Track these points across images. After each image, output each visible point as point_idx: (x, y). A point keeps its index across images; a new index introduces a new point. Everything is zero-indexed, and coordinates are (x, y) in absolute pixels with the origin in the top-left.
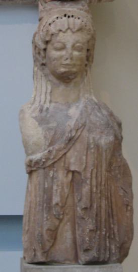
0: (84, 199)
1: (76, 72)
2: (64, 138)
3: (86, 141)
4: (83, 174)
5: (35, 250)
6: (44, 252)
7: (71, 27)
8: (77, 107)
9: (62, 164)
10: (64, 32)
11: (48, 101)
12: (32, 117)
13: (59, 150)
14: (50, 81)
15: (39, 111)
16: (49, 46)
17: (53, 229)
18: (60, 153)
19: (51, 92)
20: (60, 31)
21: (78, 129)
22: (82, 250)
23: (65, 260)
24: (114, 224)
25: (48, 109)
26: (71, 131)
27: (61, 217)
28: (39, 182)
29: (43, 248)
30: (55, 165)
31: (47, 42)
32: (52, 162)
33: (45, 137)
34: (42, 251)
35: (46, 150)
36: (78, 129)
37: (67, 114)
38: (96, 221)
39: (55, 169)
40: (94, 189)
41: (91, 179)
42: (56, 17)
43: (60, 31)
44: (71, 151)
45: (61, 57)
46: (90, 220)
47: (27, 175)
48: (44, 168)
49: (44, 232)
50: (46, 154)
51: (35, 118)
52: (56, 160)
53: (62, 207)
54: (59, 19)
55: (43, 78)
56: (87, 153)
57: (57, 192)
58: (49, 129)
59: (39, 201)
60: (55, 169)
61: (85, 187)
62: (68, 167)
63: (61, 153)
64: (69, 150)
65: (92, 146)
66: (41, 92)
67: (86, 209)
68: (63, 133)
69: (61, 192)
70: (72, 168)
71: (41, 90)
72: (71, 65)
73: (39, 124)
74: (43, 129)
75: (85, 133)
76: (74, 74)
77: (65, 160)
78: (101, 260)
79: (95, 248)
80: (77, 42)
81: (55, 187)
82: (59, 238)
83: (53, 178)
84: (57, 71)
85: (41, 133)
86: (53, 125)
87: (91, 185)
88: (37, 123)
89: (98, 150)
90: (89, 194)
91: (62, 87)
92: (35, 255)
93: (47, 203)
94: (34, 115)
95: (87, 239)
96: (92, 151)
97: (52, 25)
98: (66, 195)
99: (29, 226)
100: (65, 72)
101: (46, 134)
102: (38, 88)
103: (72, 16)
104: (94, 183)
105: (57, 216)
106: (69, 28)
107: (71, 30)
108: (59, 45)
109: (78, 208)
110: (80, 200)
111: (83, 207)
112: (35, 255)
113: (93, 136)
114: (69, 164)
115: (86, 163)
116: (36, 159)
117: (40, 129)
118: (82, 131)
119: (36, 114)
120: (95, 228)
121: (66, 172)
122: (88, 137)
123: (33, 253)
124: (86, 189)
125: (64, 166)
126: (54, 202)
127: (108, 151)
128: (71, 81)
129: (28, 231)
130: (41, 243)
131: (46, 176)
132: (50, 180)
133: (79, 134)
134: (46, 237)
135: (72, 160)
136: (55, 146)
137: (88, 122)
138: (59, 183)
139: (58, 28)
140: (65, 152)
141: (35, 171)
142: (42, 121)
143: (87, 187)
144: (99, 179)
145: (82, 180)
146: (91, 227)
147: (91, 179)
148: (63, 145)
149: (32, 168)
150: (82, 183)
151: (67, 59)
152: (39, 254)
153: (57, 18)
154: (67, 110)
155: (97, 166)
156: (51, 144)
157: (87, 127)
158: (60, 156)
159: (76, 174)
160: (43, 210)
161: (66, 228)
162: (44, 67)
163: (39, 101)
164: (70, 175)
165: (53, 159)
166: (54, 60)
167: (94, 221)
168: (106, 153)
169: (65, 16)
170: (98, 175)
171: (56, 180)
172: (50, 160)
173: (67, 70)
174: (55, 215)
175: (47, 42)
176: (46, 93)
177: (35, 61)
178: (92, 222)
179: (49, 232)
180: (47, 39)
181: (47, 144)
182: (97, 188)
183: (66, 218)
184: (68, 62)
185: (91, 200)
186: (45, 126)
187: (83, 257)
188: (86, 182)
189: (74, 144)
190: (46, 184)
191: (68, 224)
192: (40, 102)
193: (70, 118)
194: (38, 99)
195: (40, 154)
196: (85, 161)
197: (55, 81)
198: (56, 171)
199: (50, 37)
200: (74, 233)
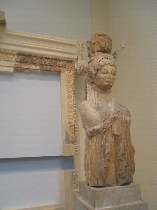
0: (121, 150)
2: (111, 117)
5: (97, 180)
6: (103, 181)
7: (110, 63)
8: (111, 103)
9: (110, 131)
10: (107, 65)
12: (92, 107)
13: (109, 124)
14: (96, 90)
16: (99, 72)
19: (97, 96)
20: (105, 64)
26: (113, 114)
28: (98, 141)
30: (107, 132)
31: (98, 70)
32: (106, 130)
33: (101, 117)
37: (108, 106)
42: (102, 58)
43: (105, 64)
44: (114, 124)
45: (106, 77)
46: (125, 161)
48: (101, 134)
49: (103, 169)
52: (107, 129)
54: (103, 59)
55: (92, 89)
58: (103, 113)
60: (107, 134)
61: (121, 143)
62: (114, 133)
63: (109, 125)
64: (113, 123)
67: (122, 155)
68: (109, 115)
70: (115, 133)
72: (110, 82)
73: (97, 111)
74: (99, 113)
75: (120, 115)
77: (111, 130)
79: (127, 176)
80: (113, 71)
81: (107, 144)
82: (109, 172)
83: (106, 139)
85: (98, 115)
87: (124, 142)
88: (95, 110)
89: (126, 124)
91: (103, 94)
92: (98, 182)
95: (124, 171)
96: (124, 124)
97: (101, 62)
99: (91, 166)
100: (107, 85)
103: (109, 59)
104: (125, 142)
106: (109, 63)
107: (110, 64)
108: (105, 71)
109: (119, 155)
110: (119, 151)
112: (98, 182)
114: (114, 131)
116: (97, 129)
117: (98, 113)
121: (112, 135)
124: (122, 145)
129: (90, 168)
131: (102, 138)
132: (104, 140)
135: (115, 129)
138: (109, 141)
139: (104, 63)
141: (96, 135)
142: (98, 109)
143: (122, 144)
146: (125, 164)
147: (124, 139)
151: (109, 78)
153: (102, 59)
154: (107, 104)
156: (104, 121)
159: (117, 137)
162: (93, 84)
165: (106, 128)
166: (102, 79)
169: (106, 58)
171: (107, 140)
173: (108, 84)
174: (107, 159)
175: (98, 70)
176: (95, 96)
179: (105, 168)
180: (99, 68)
181: (103, 121)
184: (109, 80)
185: (125, 151)
187: (122, 181)
189: (115, 121)
193: (110, 108)
195: (99, 126)
197: (99, 90)
198: (107, 135)
199: (100, 67)
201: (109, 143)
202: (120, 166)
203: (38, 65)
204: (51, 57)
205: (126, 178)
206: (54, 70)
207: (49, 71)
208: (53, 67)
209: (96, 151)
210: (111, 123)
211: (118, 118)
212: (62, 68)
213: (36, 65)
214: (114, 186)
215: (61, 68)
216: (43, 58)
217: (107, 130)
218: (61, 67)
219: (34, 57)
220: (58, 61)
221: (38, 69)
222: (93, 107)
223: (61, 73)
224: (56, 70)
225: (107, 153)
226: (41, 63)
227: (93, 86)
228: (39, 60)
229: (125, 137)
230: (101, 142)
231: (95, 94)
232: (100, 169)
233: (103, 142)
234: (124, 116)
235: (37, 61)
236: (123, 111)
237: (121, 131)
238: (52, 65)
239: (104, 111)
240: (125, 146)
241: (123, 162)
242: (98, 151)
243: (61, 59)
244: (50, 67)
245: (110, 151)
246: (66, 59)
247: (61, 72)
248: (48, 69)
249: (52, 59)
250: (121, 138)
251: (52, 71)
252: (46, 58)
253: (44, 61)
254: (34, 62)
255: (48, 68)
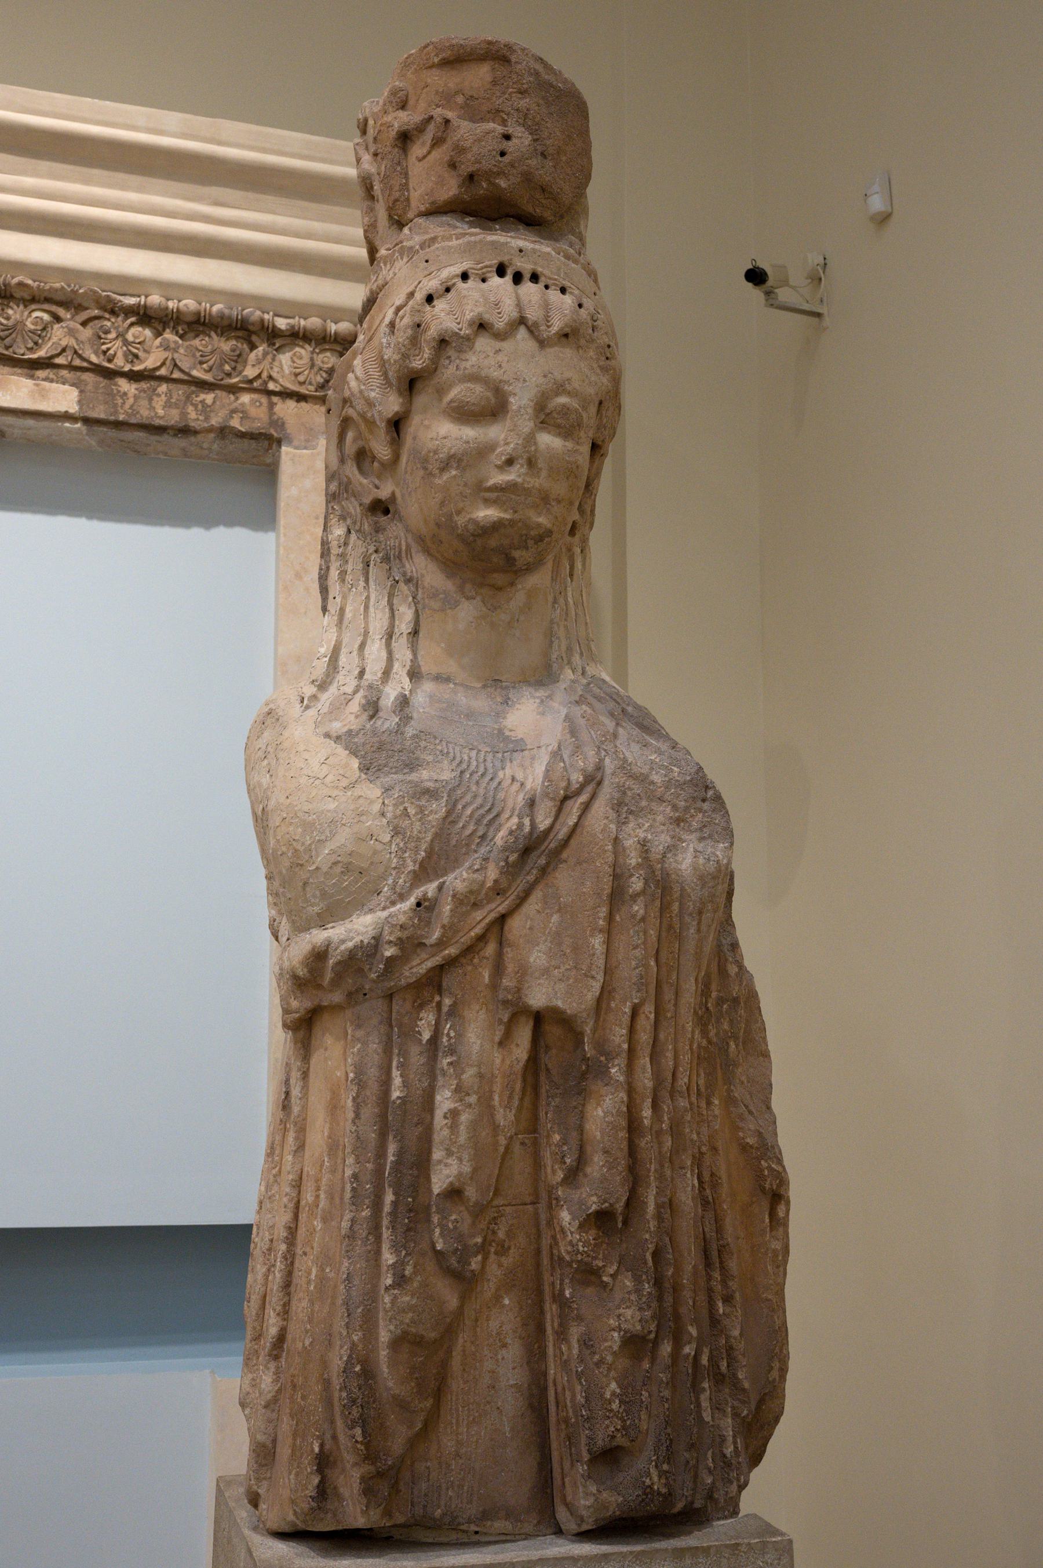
0: (596, 1166)
1: (549, 533)
2: (500, 837)
3: (611, 859)
4: (588, 1029)
11: (400, 671)
12: (327, 735)
14: (408, 581)
15: (364, 708)
16: (421, 400)
17: (433, 1335)
18: (478, 915)
19: (415, 633)
21: (566, 798)
22: (586, 1457)
23: (486, 1515)
24: (728, 1299)
25: (404, 702)
26: (531, 803)
27: (475, 1263)
28: (360, 1070)
29: (370, 1454)
32: (437, 960)
33: (397, 832)
34: (368, 1468)
35: (402, 897)
36: (566, 798)
37: (500, 731)
38: (658, 1283)
39: (447, 1002)
40: (647, 1113)
41: (631, 1051)
44: (533, 906)
47: (282, 1036)
50: (402, 919)
51: (346, 740)
52: (452, 951)
53: (478, 1211)
56: (610, 918)
57: (454, 1127)
59: (355, 1176)
62: (519, 990)
63: (481, 918)
65: (636, 884)
66: (366, 633)
69: (474, 1126)
70: (538, 997)
71: (367, 623)
72: (527, 492)
73: (365, 768)
76: (540, 539)
77: (500, 955)
78: (679, 1506)
79: (651, 1442)
81: (444, 1100)
82: (455, 1385)
84: (460, 520)
85: (376, 807)
86: (437, 773)
87: (631, 1091)
88: (355, 763)
89: (664, 908)
90: (623, 1134)
91: (467, 611)
92: (323, 1493)
93: (395, 1180)
94: (337, 727)
95: (613, 1385)
96: (638, 908)
98: (503, 1141)
99: (285, 1312)
100: (496, 526)
101: (405, 813)
102: (348, 615)
104: (645, 1080)
105: (453, 1262)
109: (565, 1216)
111: (594, 1207)
113: (642, 835)
114: (523, 971)
115: (608, 971)
116: (350, 945)
117: (372, 791)
118: (586, 807)
119: (351, 717)
120: (653, 1327)
122: (616, 840)
123: (316, 1480)
124: (602, 1112)
125: (494, 986)
126: (439, 1182)
127: (707, 916)
128: (512, 584)
130: (363, 1422)
131: (395, 1036)
132: (417, 1058)
133: (572, 821)
134: (389, 1377)
135: (537, 957)
136: (449, 878)
137: (609, 764)
138: (469, 1075)
140: (502, 909)
141: (336, 1009)
143: (608, 1102)
144: (668, 1061)
145: (585, 1059)
146: (630, 1316)
148: (492, 874)
149: (319, 996)
150: (583, 1076)
152: (350, 1480)
154: (499, 715)
155: (660, 990)
156: (424, 872)
157: (607, 791)
158: (478, 930)
159: (553, 1032)
160: (375, 1229)
161: (494, 1325)
162: (383, 519)
163: (356, 672)
164: (524, 1035)
165: (441, 944)
167: (647, 1287)
168: (699, 923)
170: (662, 1036)
172: (424, 956)
174: (438, 1254)
176: (389, 635)
177: (332, 497)
178: (638, 1291)
181: (411, 866)
182: (655, 1106)
183: (495, 1272)
186: (400, 777)
188: (602, 1072)
189: (544, 871)
190: (397, 1080)
191: (507, 1302)
192: (362, 673)
193: (517, 747)
194: (348, 661)
196: (601, 963)
198: (453, 1012)
200: (535, 1354)
201: (458, 1090)
202: (575, 1332)
203: (64, 373)
204: (189, 304)
205: (641, 1464)
206: (215, 421)
207: (161, 430)
208: (209, 398)
209: (333, 1171)
210: (498, 891)
211: (572, 842)
212: (291, 404)
213: (41, 373)
214: (505, 1538)
215: (287, 409)
216: (113, 312)
217: (451, 963)
218: (286, 394)
219: (33, 299)
220: (253, 347)
221: (66, 416)
222: (338, 739)
223: (284, 449)
224: (235, 423)
225: (436, 1190)
226: (94, 359)
227: (381, 537)
228: (71, 332)
229: (644, 1037)
230: (386, 1084)
231: (392, 610)
232: (353, 1346)
233: (406, 1084)
234: (648, 831)
235: (58, 336)
236: (642, 779)
237: (600, 977)
238: (195, 373)
239: (447, 775)
240: (633, 1126)
241: (604, 1286)
242: (348, 1172)
243: (282, 323)
244: (179, 391)
245: (467, 1169)
246: (333, 328)
247: (279, 442)
248: (161, 406)
249: (196, 325)
250: (601, 1046)
251: (196, 432)
252: (145, 316)
253: (126, 343)
254: (20, 350)
255: (159, 404)
